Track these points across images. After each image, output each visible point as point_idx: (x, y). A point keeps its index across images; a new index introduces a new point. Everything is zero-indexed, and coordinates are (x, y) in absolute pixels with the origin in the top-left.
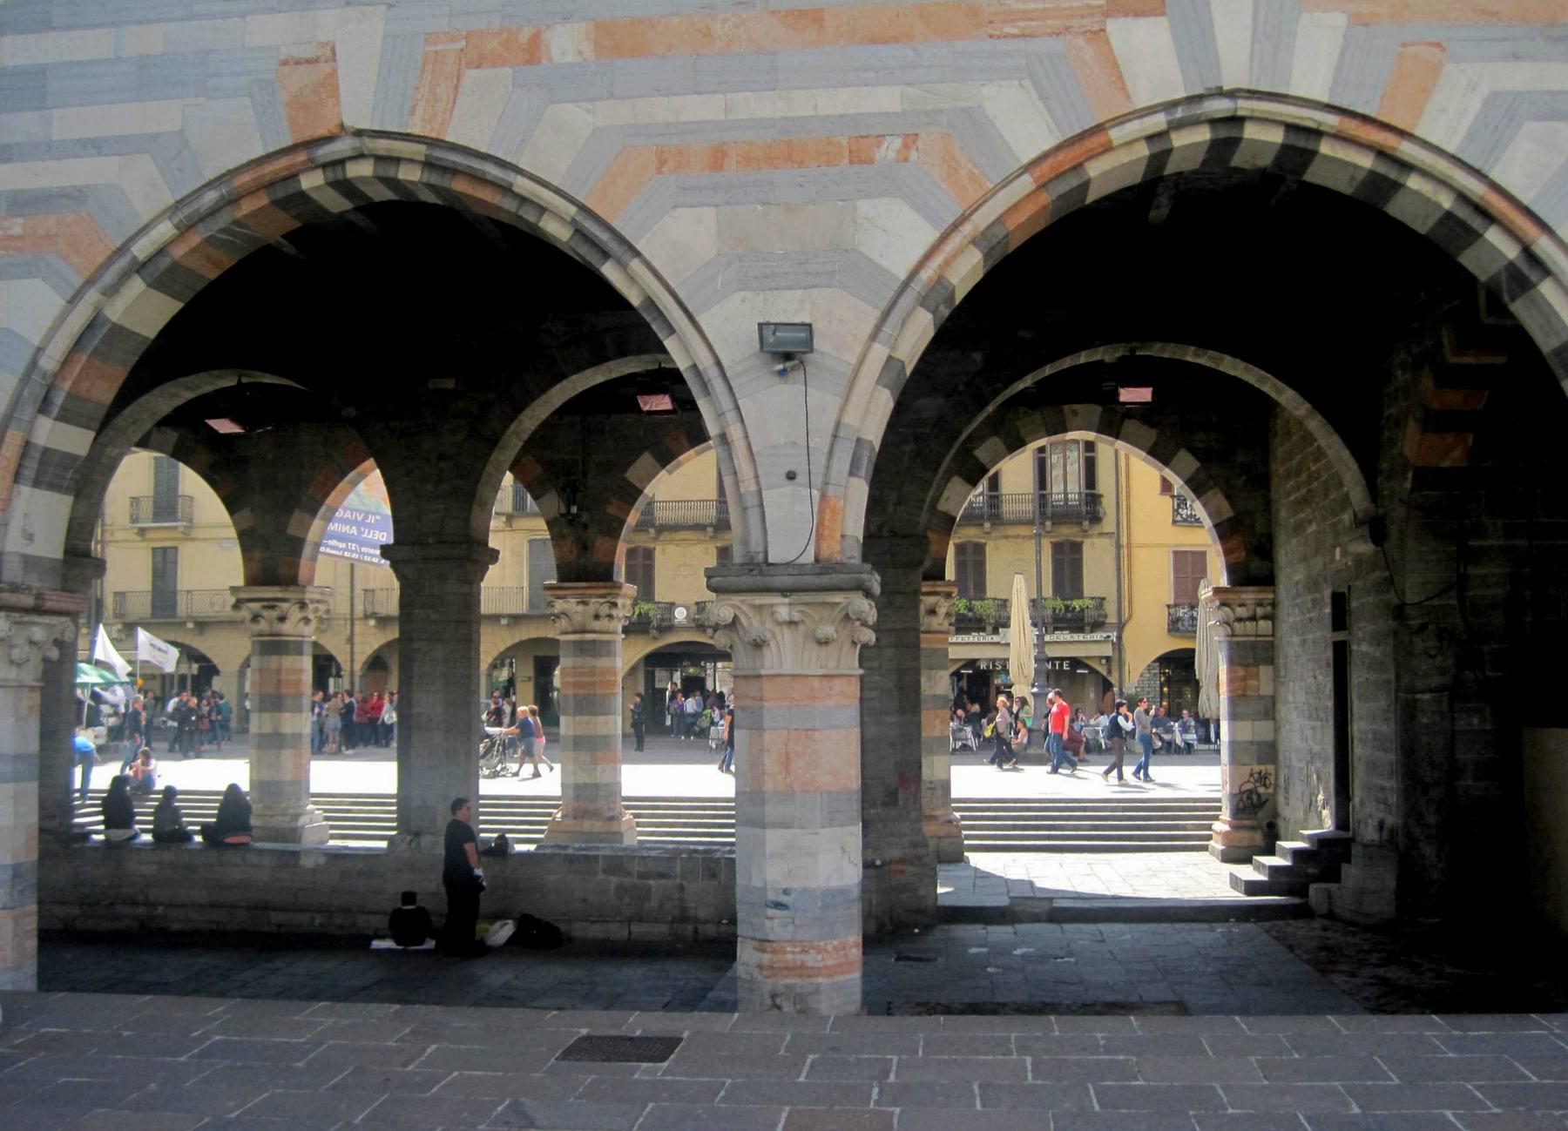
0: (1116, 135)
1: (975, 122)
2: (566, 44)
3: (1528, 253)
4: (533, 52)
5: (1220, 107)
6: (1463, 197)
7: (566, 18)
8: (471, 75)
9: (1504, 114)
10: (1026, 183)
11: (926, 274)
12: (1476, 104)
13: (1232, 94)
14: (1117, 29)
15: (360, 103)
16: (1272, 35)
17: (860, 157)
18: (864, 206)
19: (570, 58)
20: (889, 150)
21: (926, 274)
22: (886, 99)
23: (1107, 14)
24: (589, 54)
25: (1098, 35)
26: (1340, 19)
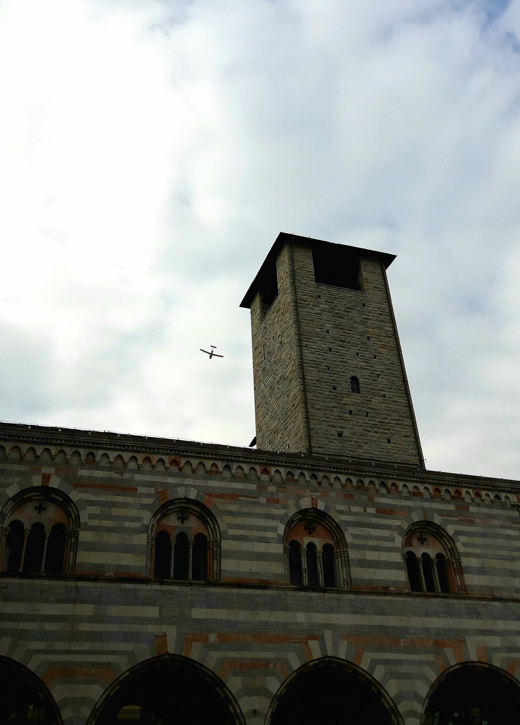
0: (310, 664)
1: (286, 661)
2: (213, 638)
3: (379, 691)
4: (206, 639)
5: (327, 659)
6: (367, 679)
7: (212, 632)
8: (194, 644)
9: (374, 663)
10: (295, 674)
11: (278, 693)
12: (369, 662)
13: (330, 657)
14: (310, 642)
15: (171, 649)
16: (335, 645)
17: (267, 667)
18: (268, 678)
19: (213, 641)
20: (272, 666)
21: (278, 693)
22: (270, 655)
23: (308, 639)
24: (217, 641)
25: (307, 644)
26: (346, 642)
